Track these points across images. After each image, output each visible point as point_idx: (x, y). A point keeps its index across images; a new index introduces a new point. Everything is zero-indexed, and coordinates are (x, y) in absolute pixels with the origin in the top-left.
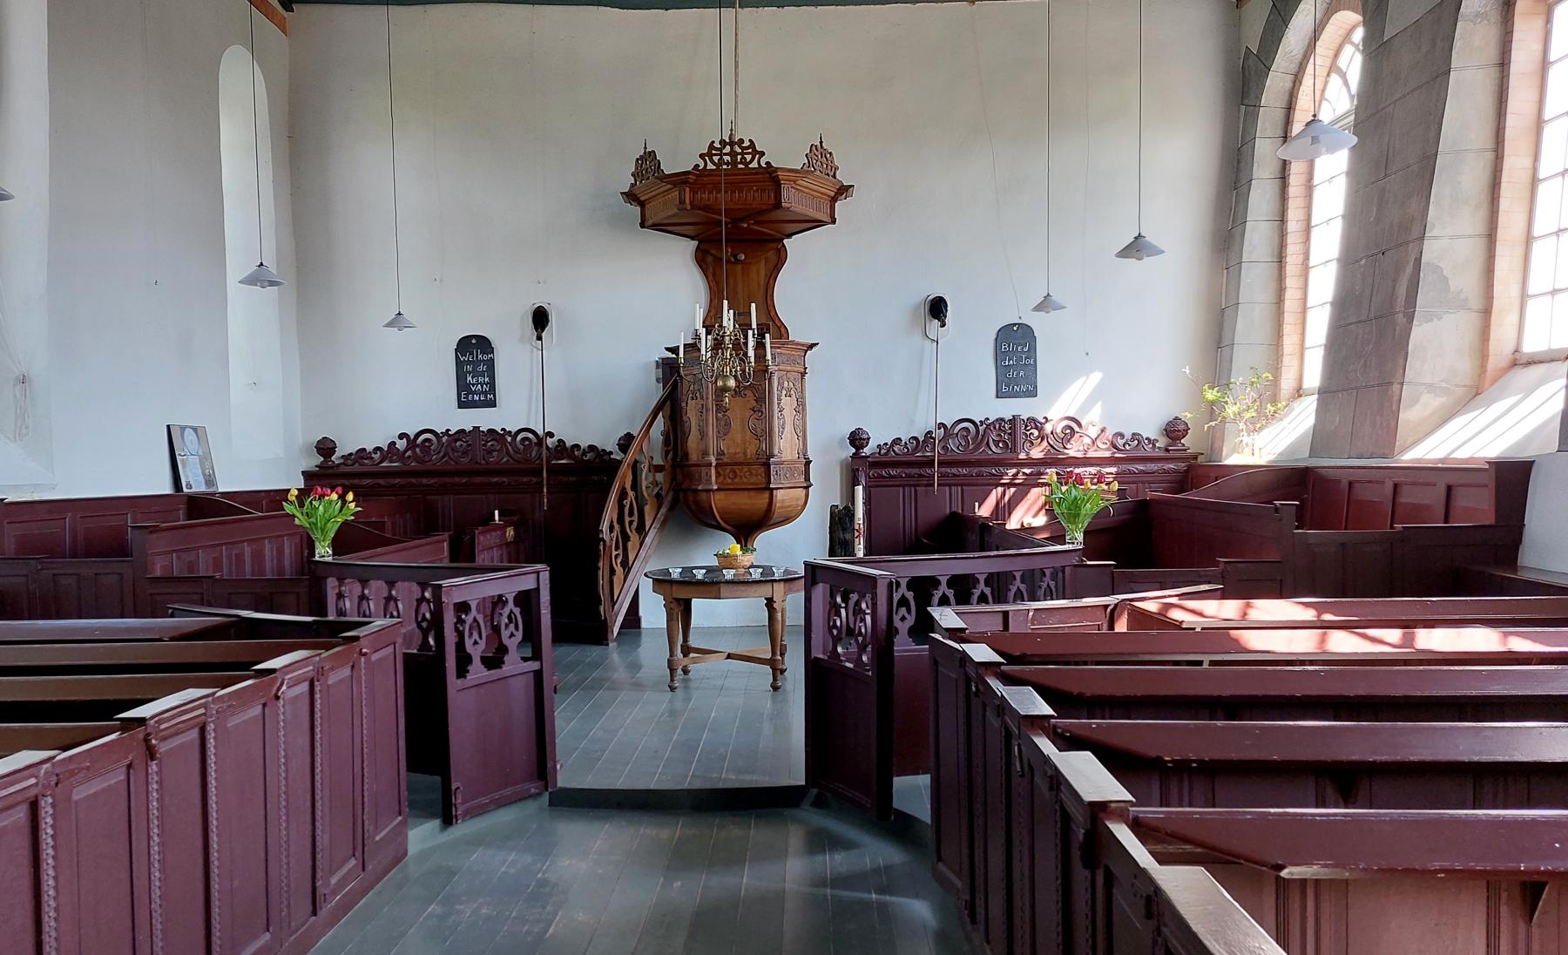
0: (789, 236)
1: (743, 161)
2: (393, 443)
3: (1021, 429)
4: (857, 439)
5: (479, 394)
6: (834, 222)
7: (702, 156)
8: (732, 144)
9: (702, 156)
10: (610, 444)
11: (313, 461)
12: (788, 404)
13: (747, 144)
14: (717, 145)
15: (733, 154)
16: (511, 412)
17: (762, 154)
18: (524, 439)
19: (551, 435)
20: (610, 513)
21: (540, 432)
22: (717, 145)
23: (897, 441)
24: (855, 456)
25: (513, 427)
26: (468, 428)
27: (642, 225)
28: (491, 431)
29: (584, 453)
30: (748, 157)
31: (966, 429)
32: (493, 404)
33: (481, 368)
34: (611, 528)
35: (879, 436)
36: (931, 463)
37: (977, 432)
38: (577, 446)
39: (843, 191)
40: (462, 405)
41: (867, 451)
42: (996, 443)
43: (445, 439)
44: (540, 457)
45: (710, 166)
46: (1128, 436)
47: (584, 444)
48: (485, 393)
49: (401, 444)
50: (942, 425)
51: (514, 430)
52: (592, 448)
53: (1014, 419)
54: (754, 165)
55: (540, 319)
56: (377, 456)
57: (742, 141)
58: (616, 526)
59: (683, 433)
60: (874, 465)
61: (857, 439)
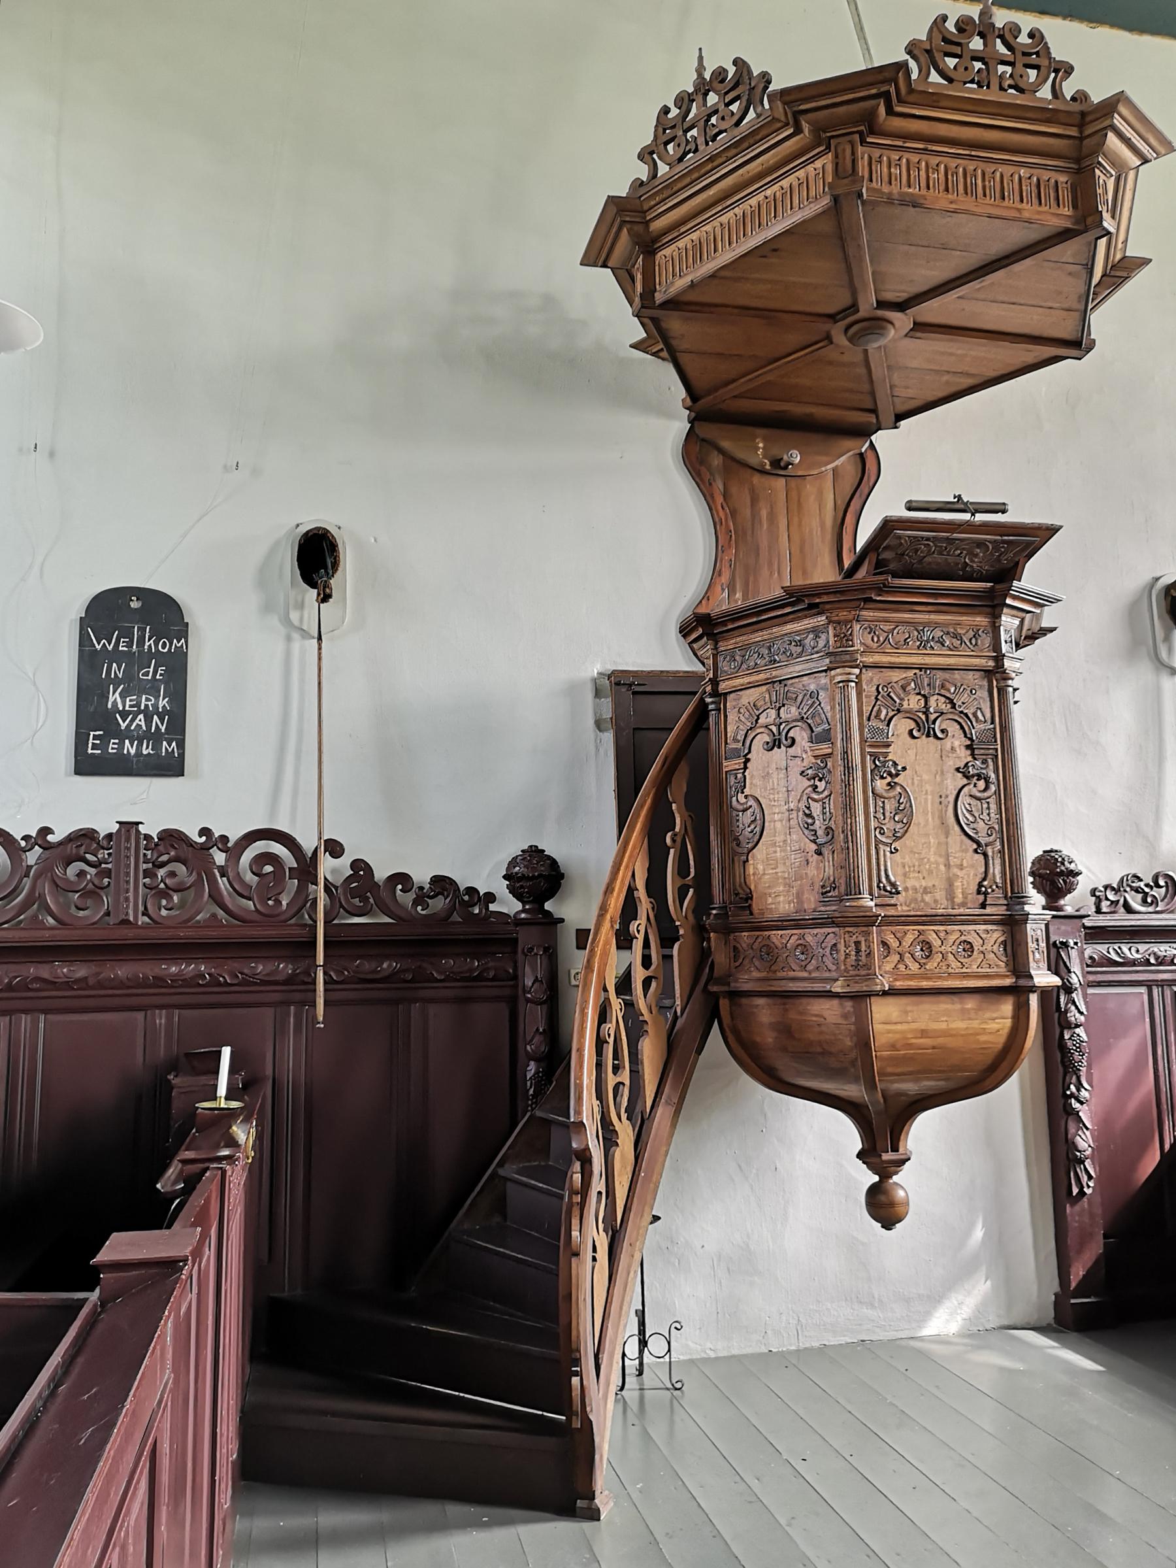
5: (140, 738)
10: (485, 874)
16: (220, 792)
19: (334, 848)
21: (308, 843)
26: (106, 826)
28: (172, 837)
29: (422, 898)
32: (173, 767)
33: (148, 673)
38: (402, 879)
40: (85, 765)
44: (304, 902)
47: (422, 876)
48: (156, 738)
51: (234, 836)
52: (442, 884)
59: (730, 838)
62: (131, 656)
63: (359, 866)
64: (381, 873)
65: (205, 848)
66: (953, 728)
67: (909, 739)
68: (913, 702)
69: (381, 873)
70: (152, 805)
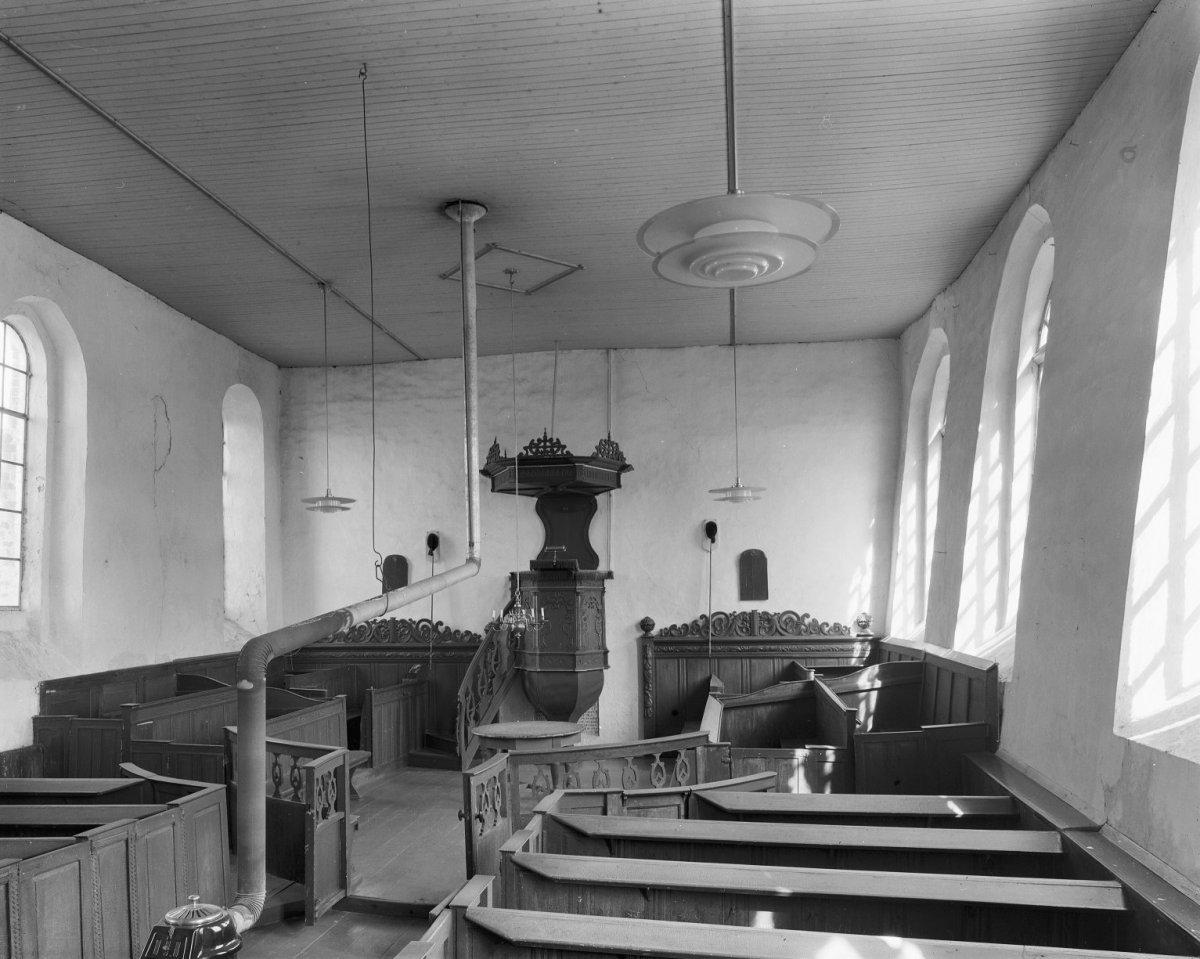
0: (598, 494)
1: (552, 451)
3: (757, 620)
4: (646, 625)
6: (619, 486)
7: (525, 448)
8: (545, 440)
9: (525, 448)
13: (555, 441)
14: (536, 442)
15: (545, 447)
17: (565, 447)
18: (424, 626)
20: (466, 683)
22: (536, 442)
24: (644, 638)
25: (416, 619)
27: (493, 490)
28: (403, 621)
29: (462, 637)
30: (549, 449)
31: (720, 619)
34: (467, 695)
35: (661, 624)
37: (727, 621)
38: (457, 631)
39: (625, 468)
41: (654, 632)
45: (530, 454)
46: (831, 624)
47: (463, 630)
52: (468, 633)
53: (754, 612)
54: (559, 453)
57: (551, 440)
58: (471, 694)
60: (657, 643)
61: (646, 625)
62: (395, 572)
63: (447, 628)
64: (452, 631)
65: (410, 625)
69: (452, 631)
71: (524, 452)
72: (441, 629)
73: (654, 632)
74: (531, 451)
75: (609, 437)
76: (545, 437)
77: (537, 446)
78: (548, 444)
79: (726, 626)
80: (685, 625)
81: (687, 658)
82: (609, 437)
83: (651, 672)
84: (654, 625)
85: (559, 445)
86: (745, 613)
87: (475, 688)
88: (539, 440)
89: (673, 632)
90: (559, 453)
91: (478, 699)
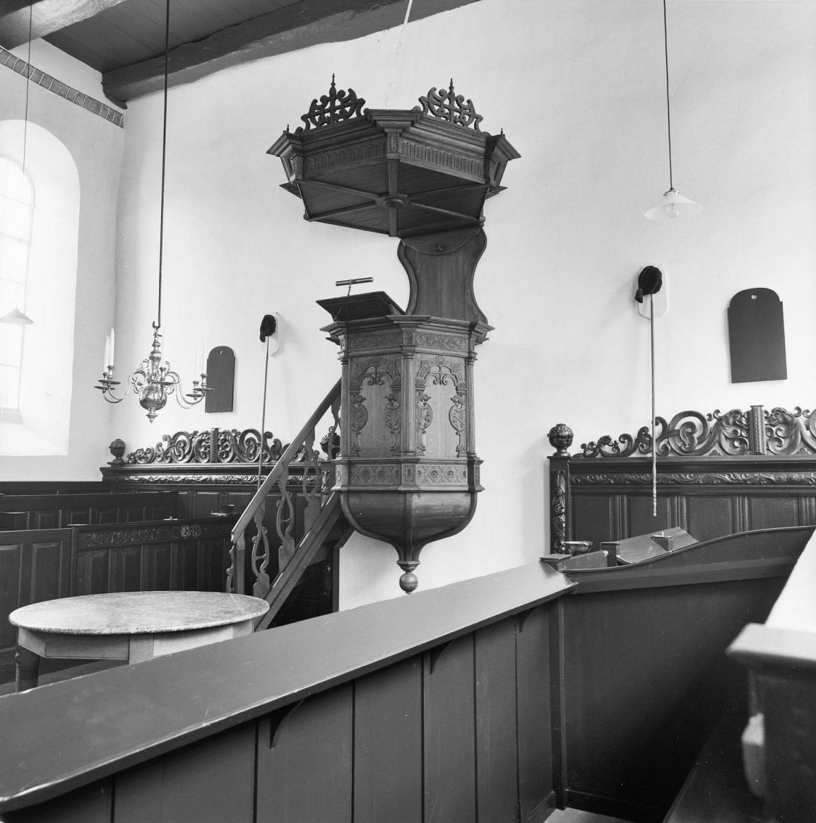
1: (343, 112)
2: (160, 445)
3: (762, 424)
4: (559, 438)
7: (304, 118)
9: (304, 118)
11: (108, 459)
12: (440, 397)
13: (347, 94)
14: (319, 103)
17: (362, 102)
23: (605, 440)
24: (555, 460)
34: (250, 530)
35: (582, 437)
36: (646, 466)
42: (731, 440)
43: (195, 441)
49: (165, 445)
50: (659, 420)
51: (242, 432)
53: (751, 415)
55: (268, 326)
56: (149, 455)
57: (342, 93)
58: (262, 531)
61: (559, 438)
63: (277, 441)
66: (449, 380)
67: (432, 383)
68: (435, 369)
70: (225, 422)
71: (303, 125)
72: (270, 443)
73: (573, 450)
74: (315, 123)
75: (451, 88)
76: (333, 90)
77: (322, 110)
78: (338, 103)
79: (701, 440)
80: (625, 437)
81: (628, 494)
82: (451, 88)
83: (563, 518)
84: (570, 437)
85: (354, 101)
86: (737, 412)
87: (268, 522)
88: (324, 99)
89: (607, 449)
90: (354, 115)
91: (275, 544)
